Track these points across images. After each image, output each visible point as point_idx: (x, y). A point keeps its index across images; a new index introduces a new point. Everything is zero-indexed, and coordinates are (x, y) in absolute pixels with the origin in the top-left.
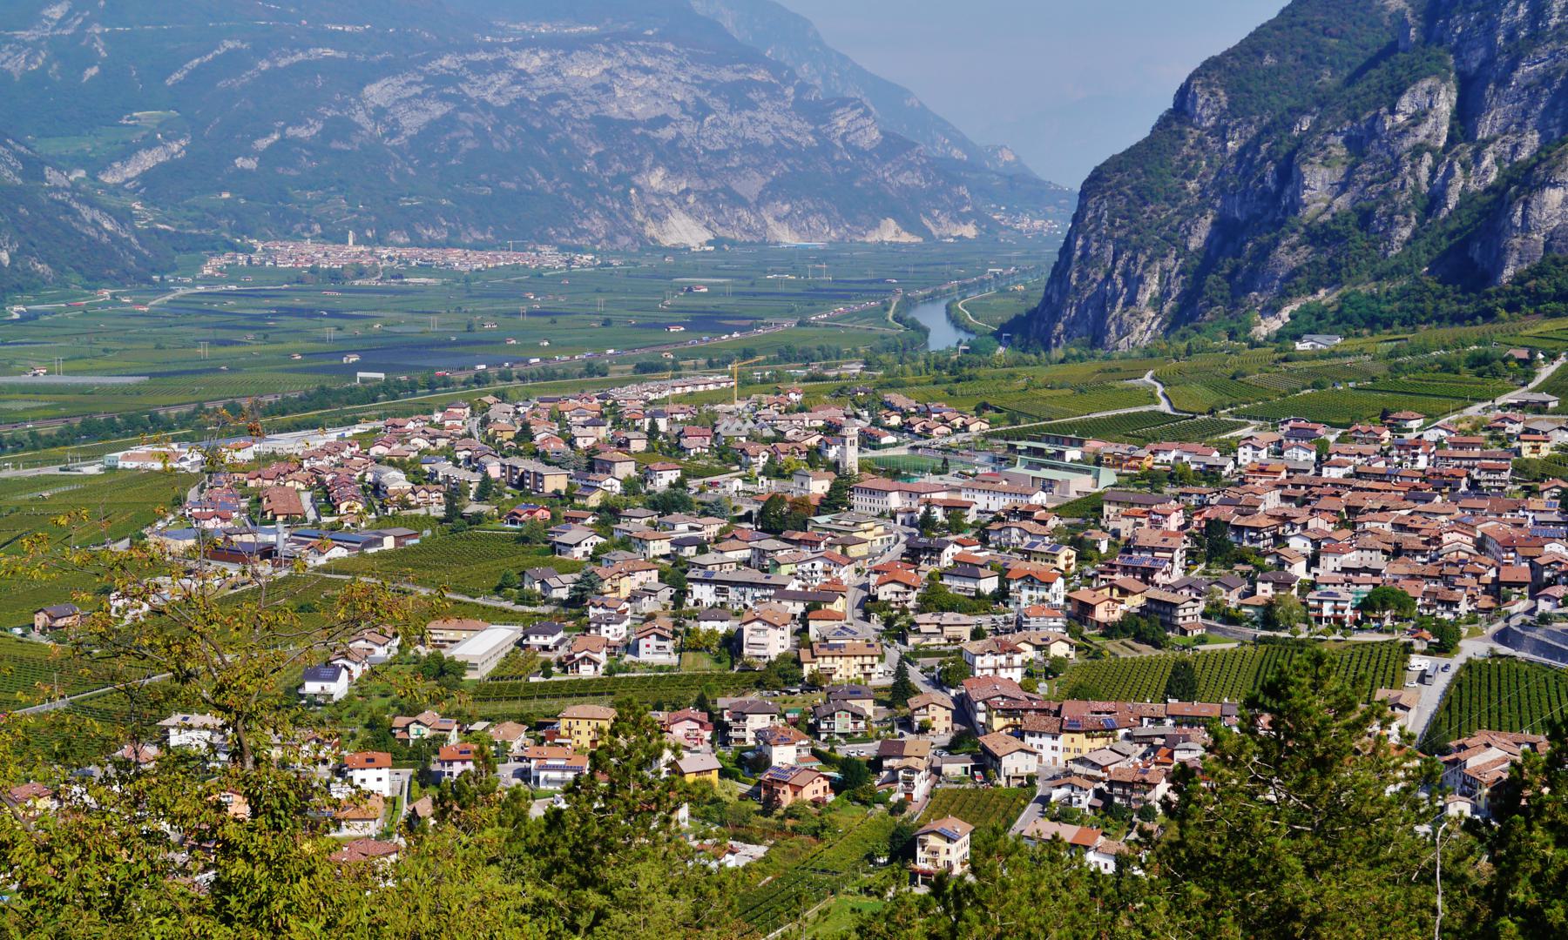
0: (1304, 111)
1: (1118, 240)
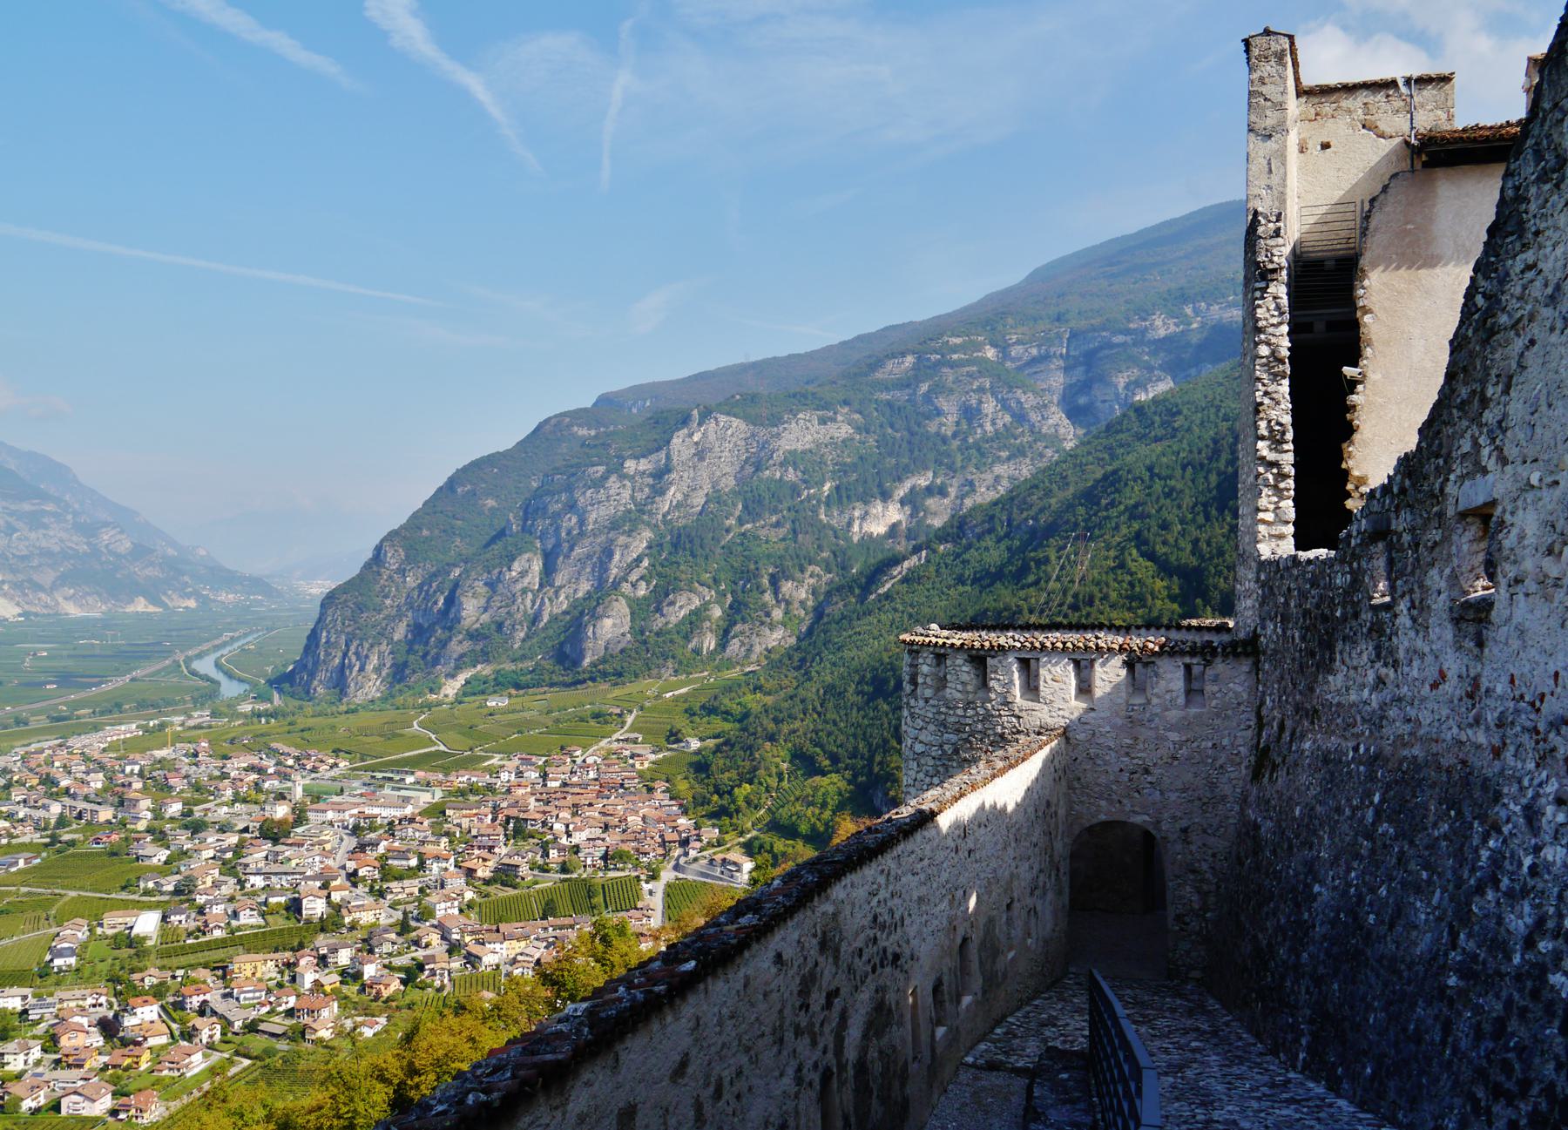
0: (455, 566)
1: (348, 633)
